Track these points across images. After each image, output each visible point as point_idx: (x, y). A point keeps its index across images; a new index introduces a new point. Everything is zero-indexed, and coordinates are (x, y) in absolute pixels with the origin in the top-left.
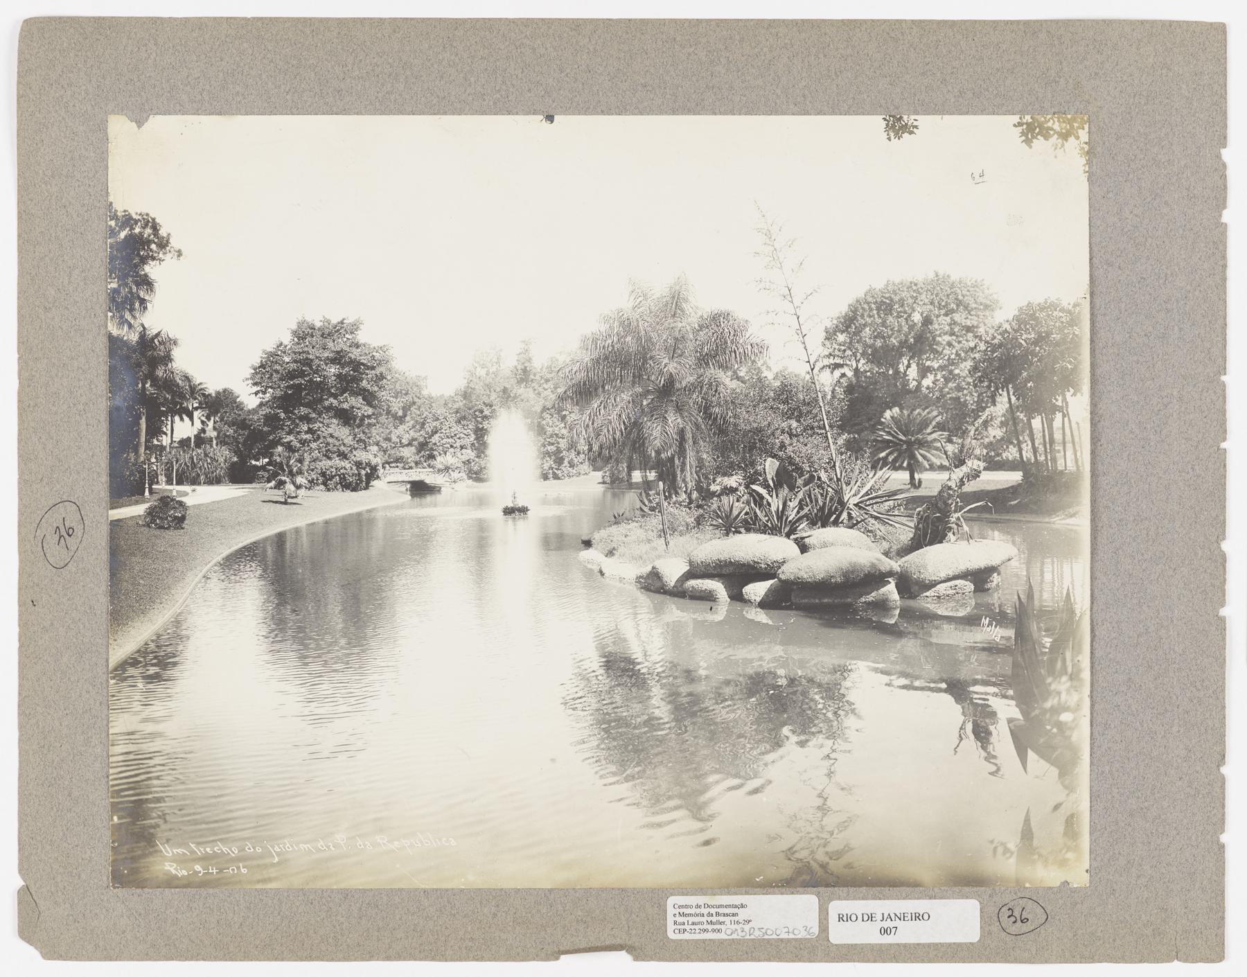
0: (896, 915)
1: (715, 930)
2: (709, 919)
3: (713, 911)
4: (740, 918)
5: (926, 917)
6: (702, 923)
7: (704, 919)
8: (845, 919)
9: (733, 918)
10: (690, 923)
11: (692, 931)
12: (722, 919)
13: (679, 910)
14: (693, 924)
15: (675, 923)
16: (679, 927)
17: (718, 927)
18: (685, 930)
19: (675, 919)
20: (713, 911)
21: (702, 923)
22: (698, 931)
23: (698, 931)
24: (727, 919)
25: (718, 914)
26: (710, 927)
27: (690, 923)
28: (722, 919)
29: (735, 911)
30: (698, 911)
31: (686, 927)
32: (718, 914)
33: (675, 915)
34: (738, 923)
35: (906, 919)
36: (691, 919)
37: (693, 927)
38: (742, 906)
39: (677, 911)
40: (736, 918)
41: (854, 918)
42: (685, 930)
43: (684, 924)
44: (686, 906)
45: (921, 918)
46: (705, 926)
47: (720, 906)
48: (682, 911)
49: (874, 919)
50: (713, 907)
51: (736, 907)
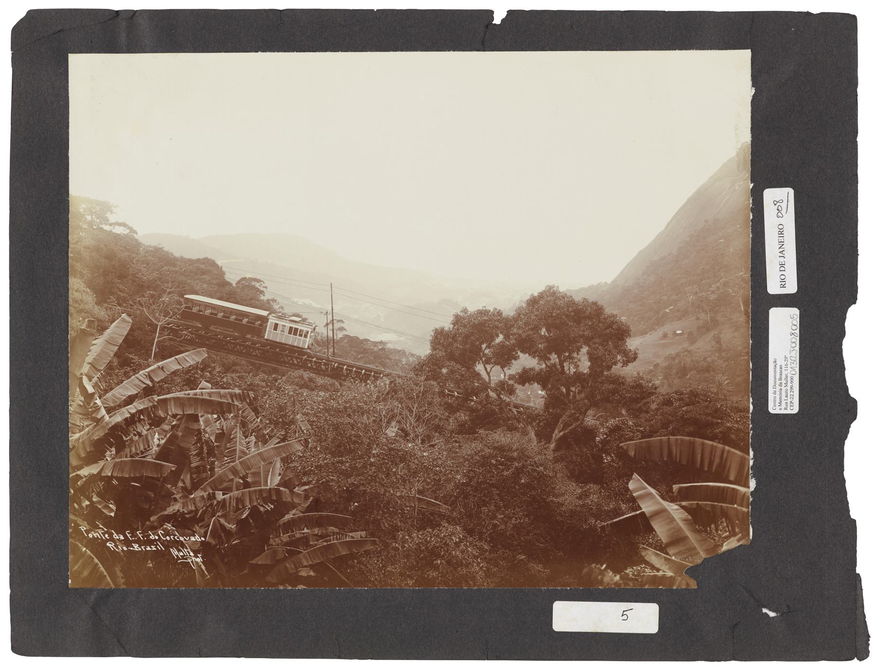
0: (780, 248)
1: (792, 381)
3: (778, 382)
4: (783, 363)
5: (781, 227)
6: (787, 390)
7: (784, 389)
8: (783, 283)
10: (786, 399)
11: (792, 397)
12: (784, 377)
13: (777, 407)
14: (787, 396)
15: (786, 409)
16: (788, 408)
18: (791, 402)
20: (778, 382)
21: (787, 390)
22: (792, 393)
23: (792, 393)
24: (784, 373)
25: (780, 379)
26: (789, 384)
27: (786, 399)
28: (784, 377)
30: (778, 393)
32: (780, 379)
33: (781, 409)
35: (782, 241)
36: (784, 398)
37: (789, 396)
39: (778, 408)
40: (783, 367)
41: (783, 277)
42: (791, 402)
44: (775, 401)
45: (781, 231)
46: (789, 388)
47: (775, 378)
48: (777, 404)
49: (783, 263)
51: (775, 366)
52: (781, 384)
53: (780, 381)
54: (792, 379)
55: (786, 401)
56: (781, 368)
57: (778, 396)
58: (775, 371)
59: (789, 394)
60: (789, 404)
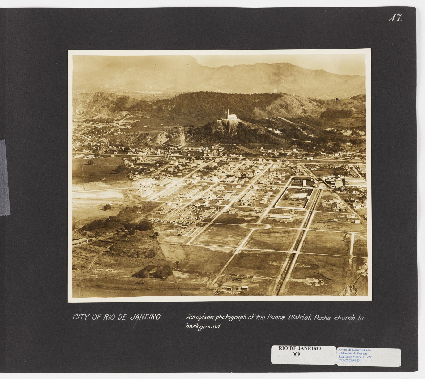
2: (354, 355)
3: (356, 352)
4: (368, 356)
6: (351, 357)
7: (352, 355)
9: (364, 355)
12: (359, 355)
14: (347, 357)
15: (340, 357)
17: (358, 359)
18: (344, 360)
19: (340, 355)
22: (349, 360)
23: (349, 360)
24: (362, 356)
25: (358, 353)
26: (354, 359)
28: (359, 355)
29: (365, 352)
30: (350, 352)
31: (344, 358)
32: (358, 353)
33: (340, 353)
34: (367, 357)
37: (347, 359)
38: (369, 351)
39: (341, 352)
40: (366, 356)
42: (344, 360)
43: (343, 357)
46: (352, 358)
47: (359, 350)
48: (343, 352)
50: (356, 350)
51: (366, 350)
52: (355, 354)
53: (357, 353)
54: (358, 360)
55: (344, 357)
56: (365, 354)
57: (347, 352)
58: (364, 350)
59: (349, 359)
60: (343, 358)
